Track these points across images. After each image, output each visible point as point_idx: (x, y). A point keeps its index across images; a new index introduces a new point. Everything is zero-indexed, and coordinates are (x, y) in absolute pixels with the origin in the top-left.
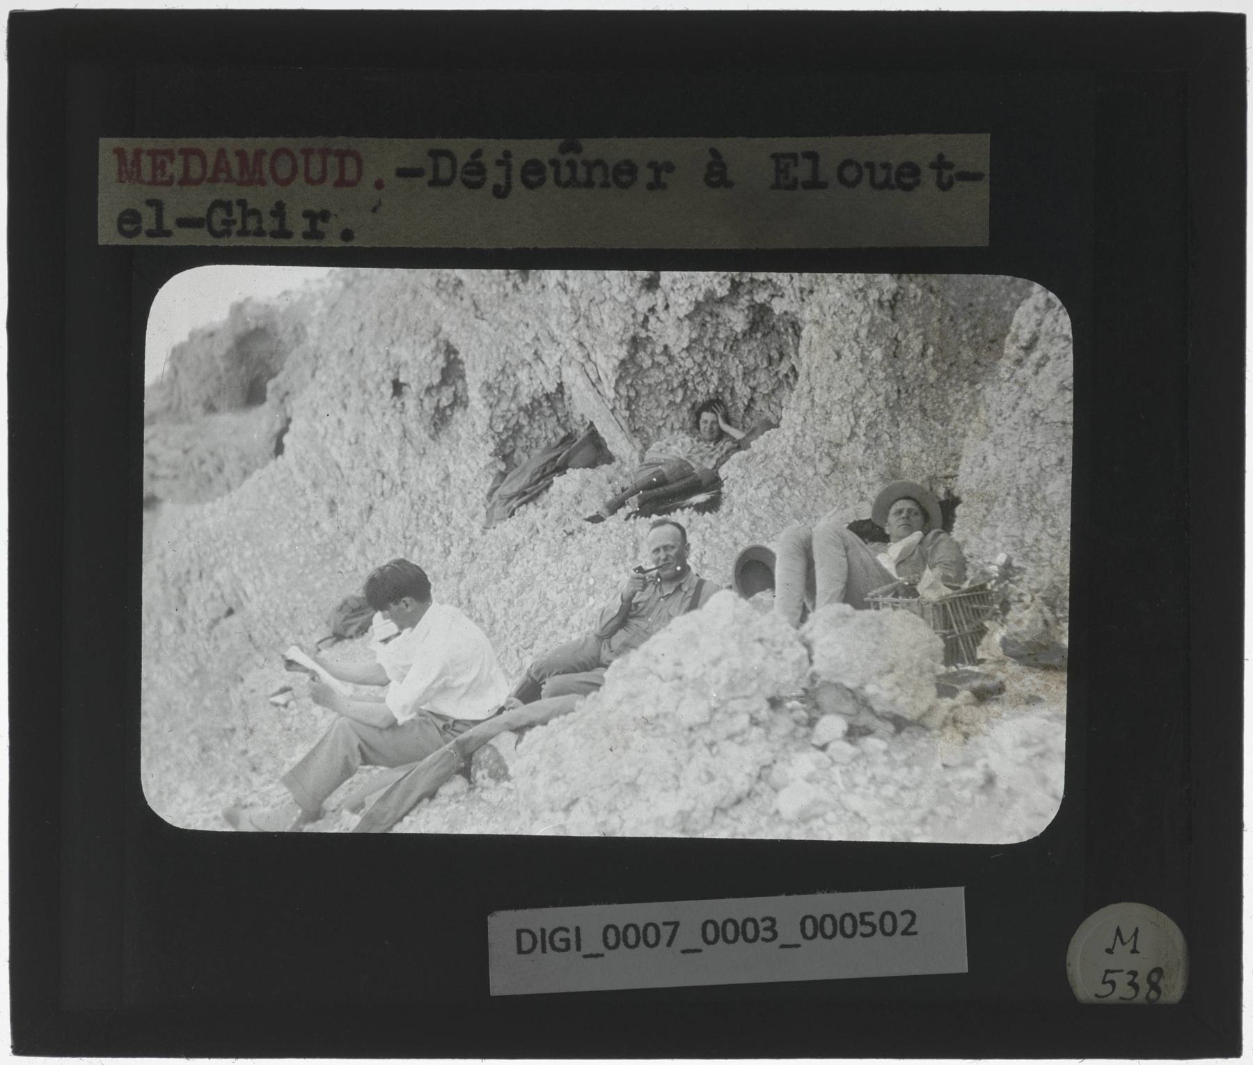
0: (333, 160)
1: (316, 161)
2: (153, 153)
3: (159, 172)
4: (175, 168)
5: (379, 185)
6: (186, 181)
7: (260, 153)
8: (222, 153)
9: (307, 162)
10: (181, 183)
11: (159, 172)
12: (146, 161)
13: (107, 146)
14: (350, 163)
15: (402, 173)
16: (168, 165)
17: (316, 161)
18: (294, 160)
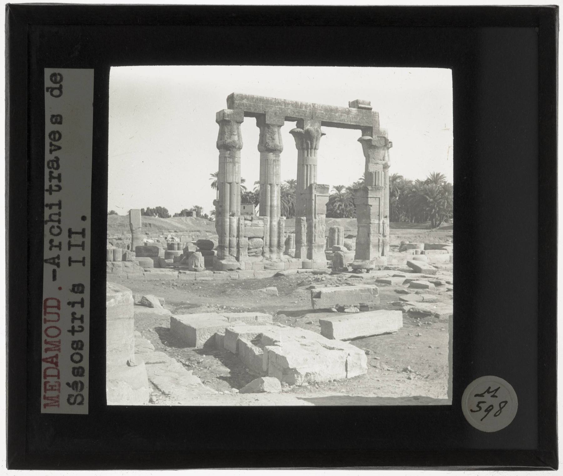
0: (49, 310)
1: (49, 317)
2: (46, 390)
3: (54, 388)
4: (52, 381)
5: (60, 288)
6: (58, 376)
7: (46, 343)
8: (46, 360)
9: (49, 321)
10: (59, 378)
11: (54, 388)
12: (49, 394)
13: (43, 411)
14: (49, 303)
15: (54, 278)
16: (50, 384)
17: (49, 317)
18: (48, 328)
